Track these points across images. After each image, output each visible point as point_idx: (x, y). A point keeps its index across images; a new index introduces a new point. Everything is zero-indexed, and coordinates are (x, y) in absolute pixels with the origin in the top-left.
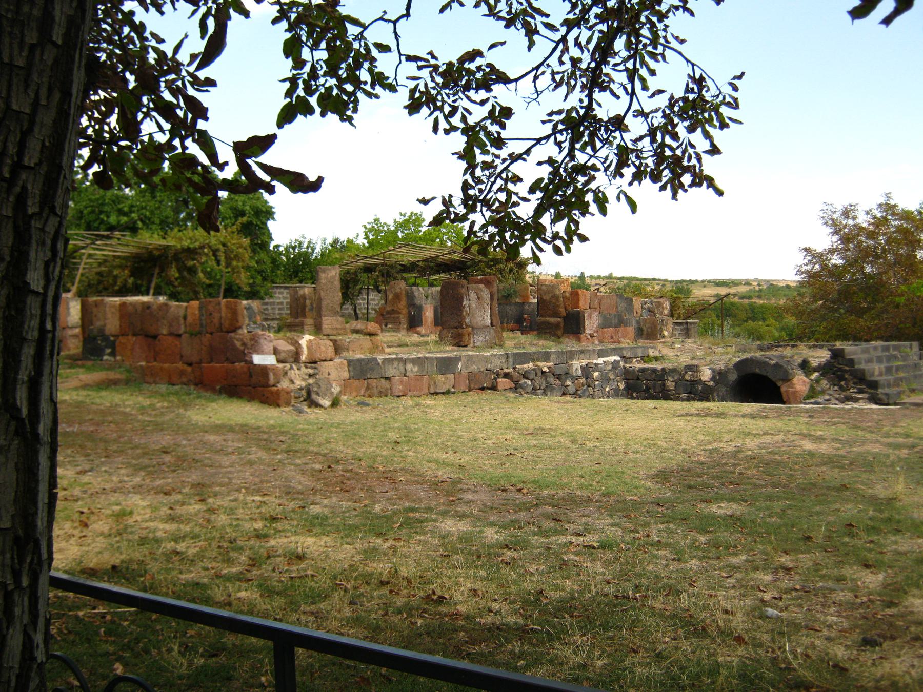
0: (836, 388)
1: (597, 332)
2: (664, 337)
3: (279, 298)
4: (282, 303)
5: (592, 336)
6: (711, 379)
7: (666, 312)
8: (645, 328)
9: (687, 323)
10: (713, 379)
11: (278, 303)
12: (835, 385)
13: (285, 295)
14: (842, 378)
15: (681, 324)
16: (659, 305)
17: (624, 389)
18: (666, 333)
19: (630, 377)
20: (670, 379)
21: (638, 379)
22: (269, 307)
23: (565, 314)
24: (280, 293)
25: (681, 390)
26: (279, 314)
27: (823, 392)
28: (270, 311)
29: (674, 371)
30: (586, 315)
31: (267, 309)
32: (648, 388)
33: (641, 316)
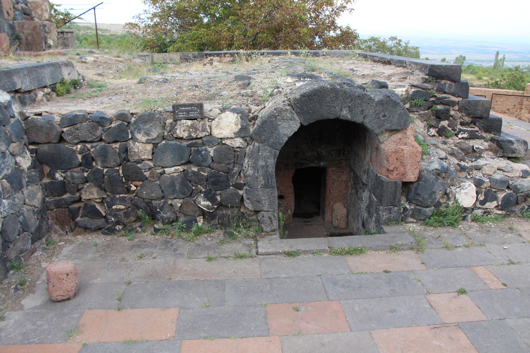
0: (433, 131)
2: (50, 47)
6: (238, 134)
8: (23, 36)
10: (242, 133)
12: (431, 126)
14: (440, 116)
17: (33, 166)
18: (51, 42)
19: (41, 138)
20: (139, 136)
21: (61, 140)
25: (168, 158)
29: (148, 118)
32: (88, 161)
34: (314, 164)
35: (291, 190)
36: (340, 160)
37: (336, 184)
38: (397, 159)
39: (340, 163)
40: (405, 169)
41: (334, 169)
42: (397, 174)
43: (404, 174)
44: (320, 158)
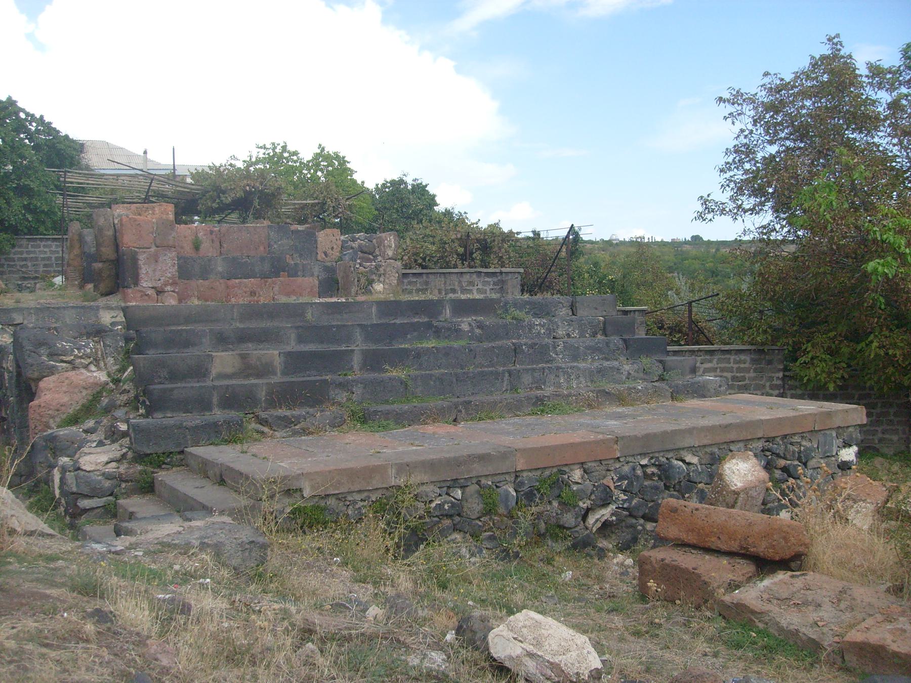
1: (174, 284)
3: (46, 252)
4: (49, 259)
5: (160, 292)
7: (390, 253)
9: (501, 273)
11: (43, 259)
13: (53, 248)
15: (494, 274)
16: (381, 242)
22: (29, 264)
23: (113, 256)
24: (45, 246)
26: (44, 271)
27: (107, 410)
28: (30, 269)
30: (142, 258)
31: (26, 266)
33: (341, 259)
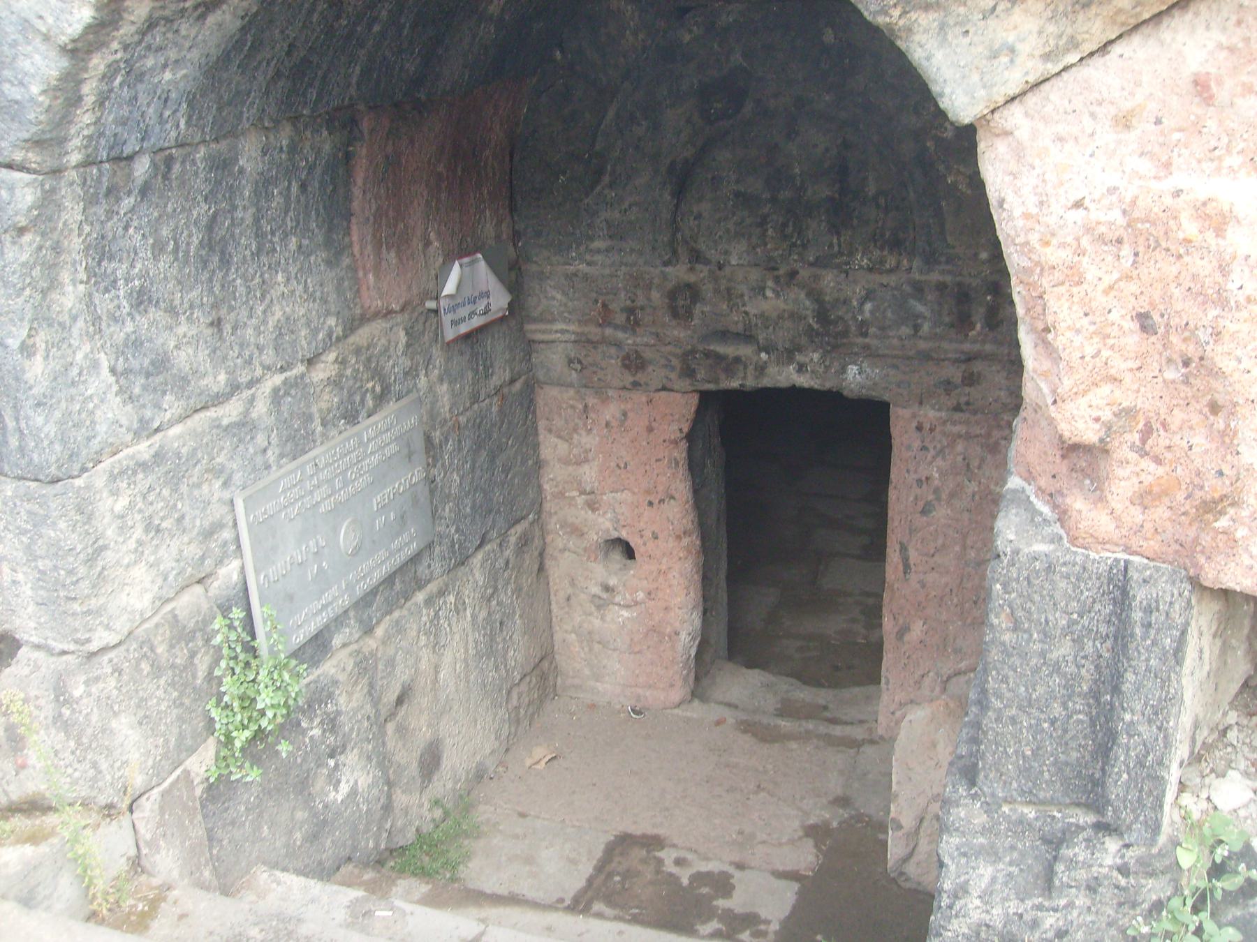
34: (801, 368)
35: (676, 514)
36: (970, 358)
37: (942, 513)
38: (1145, 322)
39: (971, 379)
40: (1226, 440)
41: (930, 414)
42: (1145, 498)
43: (1211, 507)
44: (829, 330)
